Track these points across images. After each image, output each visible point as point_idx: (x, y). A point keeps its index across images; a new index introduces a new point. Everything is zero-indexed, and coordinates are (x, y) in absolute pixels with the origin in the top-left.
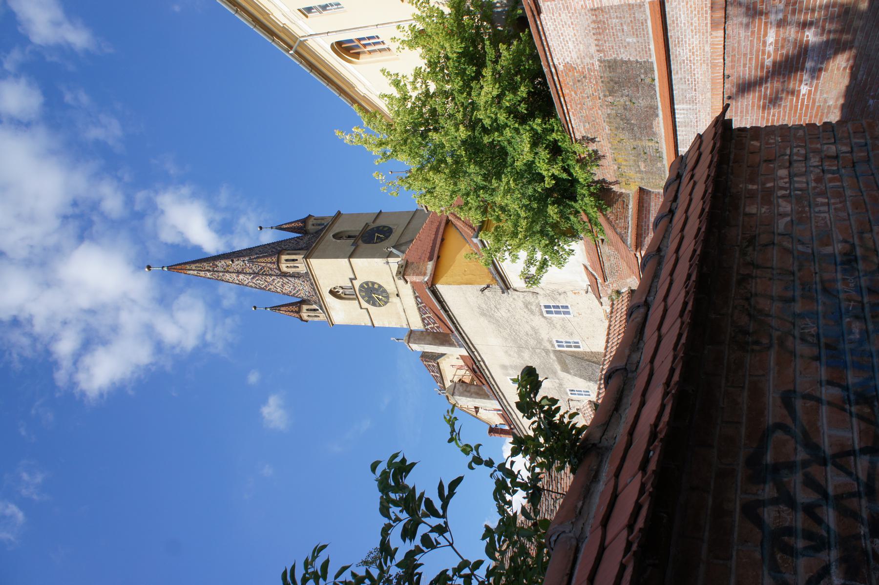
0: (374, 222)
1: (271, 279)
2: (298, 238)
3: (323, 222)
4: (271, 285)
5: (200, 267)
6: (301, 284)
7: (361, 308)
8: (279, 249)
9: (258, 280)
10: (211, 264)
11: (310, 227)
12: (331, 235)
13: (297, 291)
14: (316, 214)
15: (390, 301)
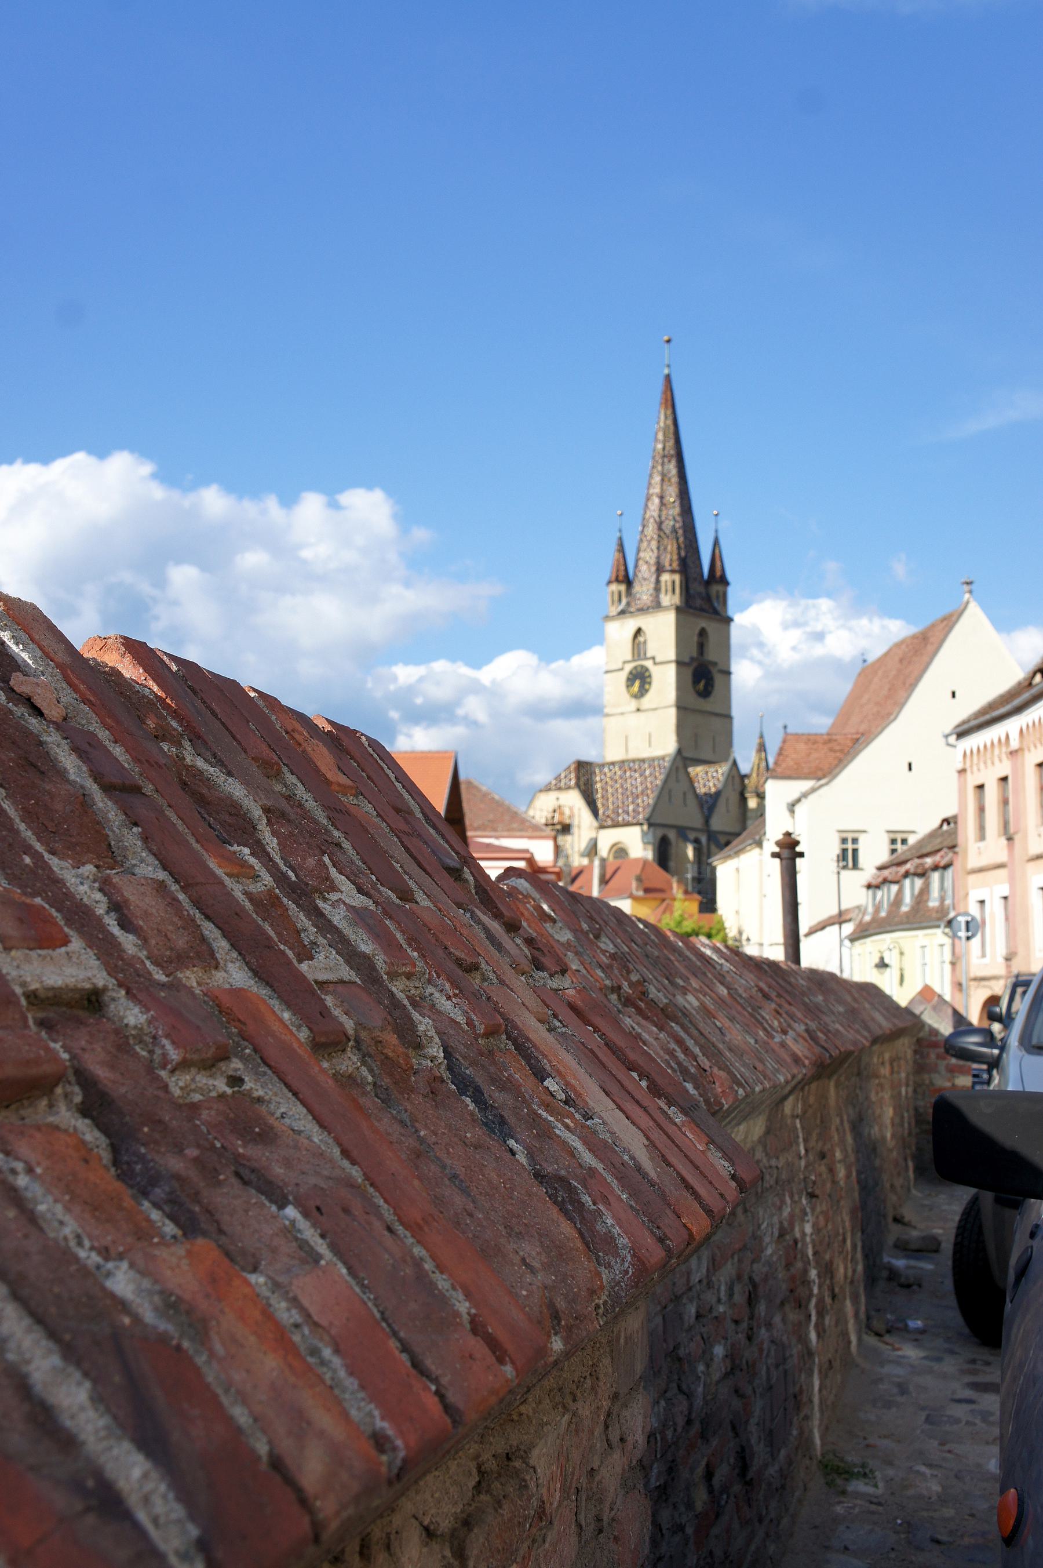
7: (625, 662)
11: (715, 588)
14: (731, 590)
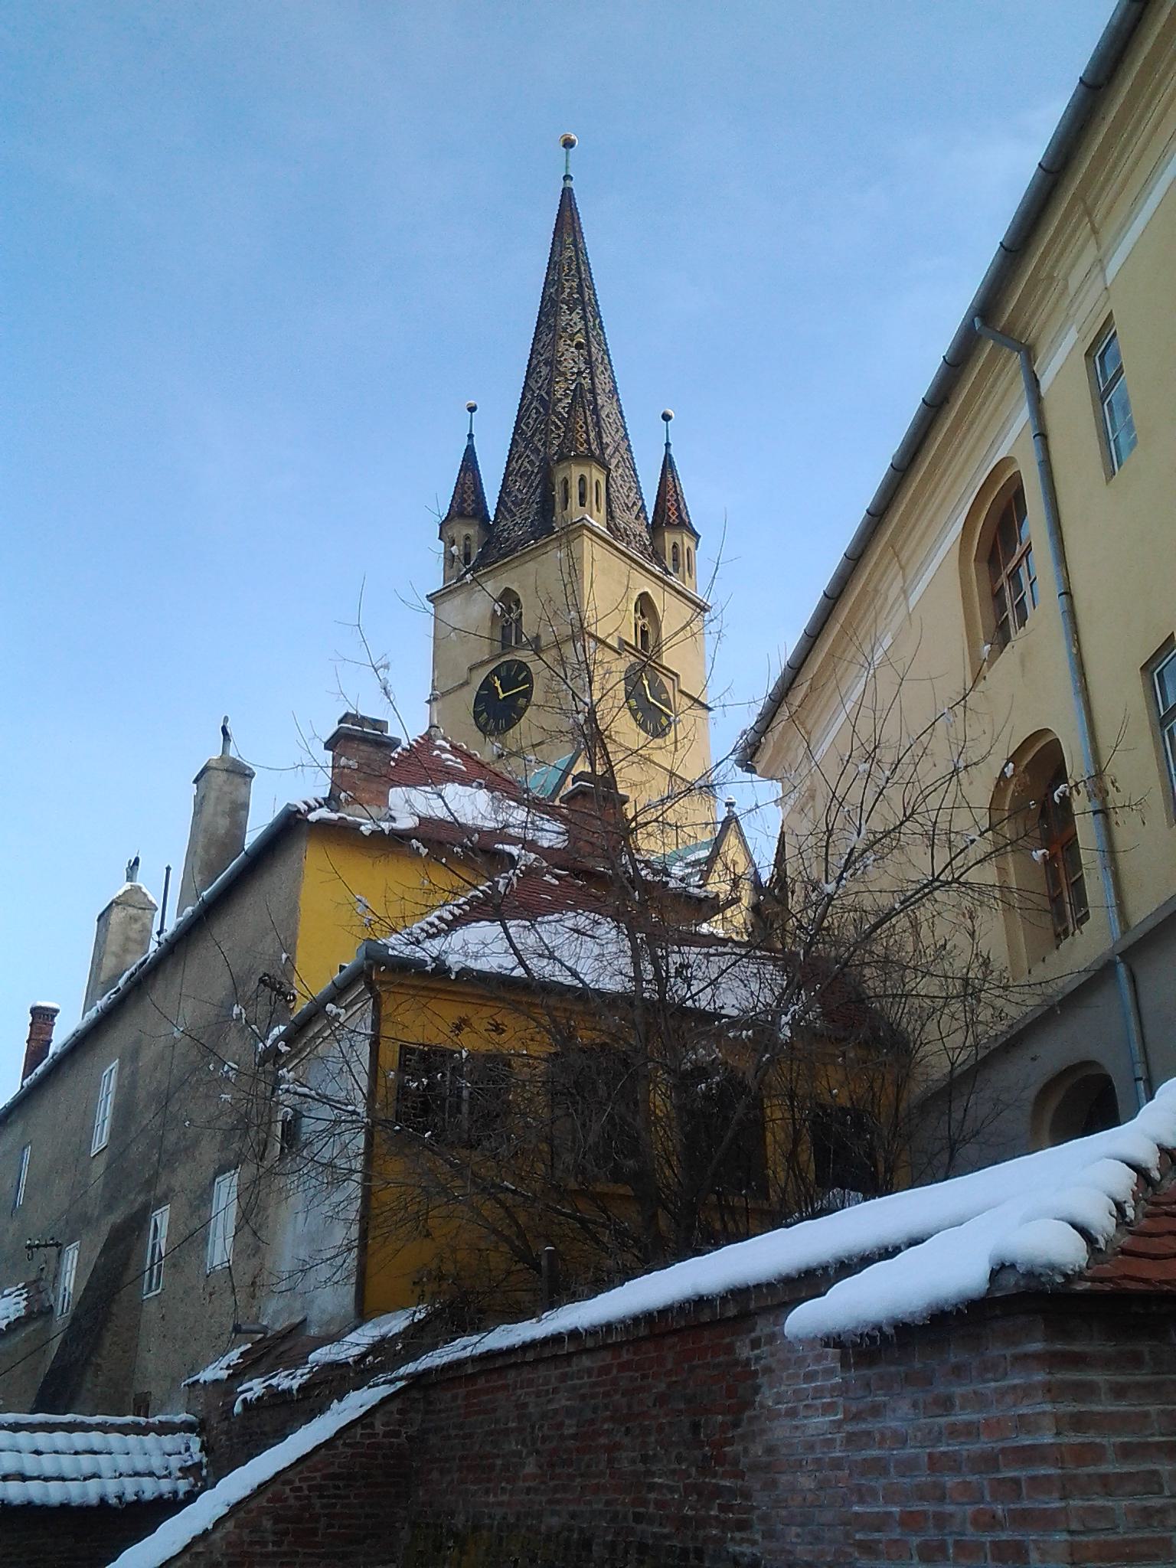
0: (681, 692)
2: (643, 508)
4: (526, 447)
5: (570, 270)
6: (526, 519)
8: (614, 462)
9: (538, 412)
12: (647, 589)
13: (510, 511)
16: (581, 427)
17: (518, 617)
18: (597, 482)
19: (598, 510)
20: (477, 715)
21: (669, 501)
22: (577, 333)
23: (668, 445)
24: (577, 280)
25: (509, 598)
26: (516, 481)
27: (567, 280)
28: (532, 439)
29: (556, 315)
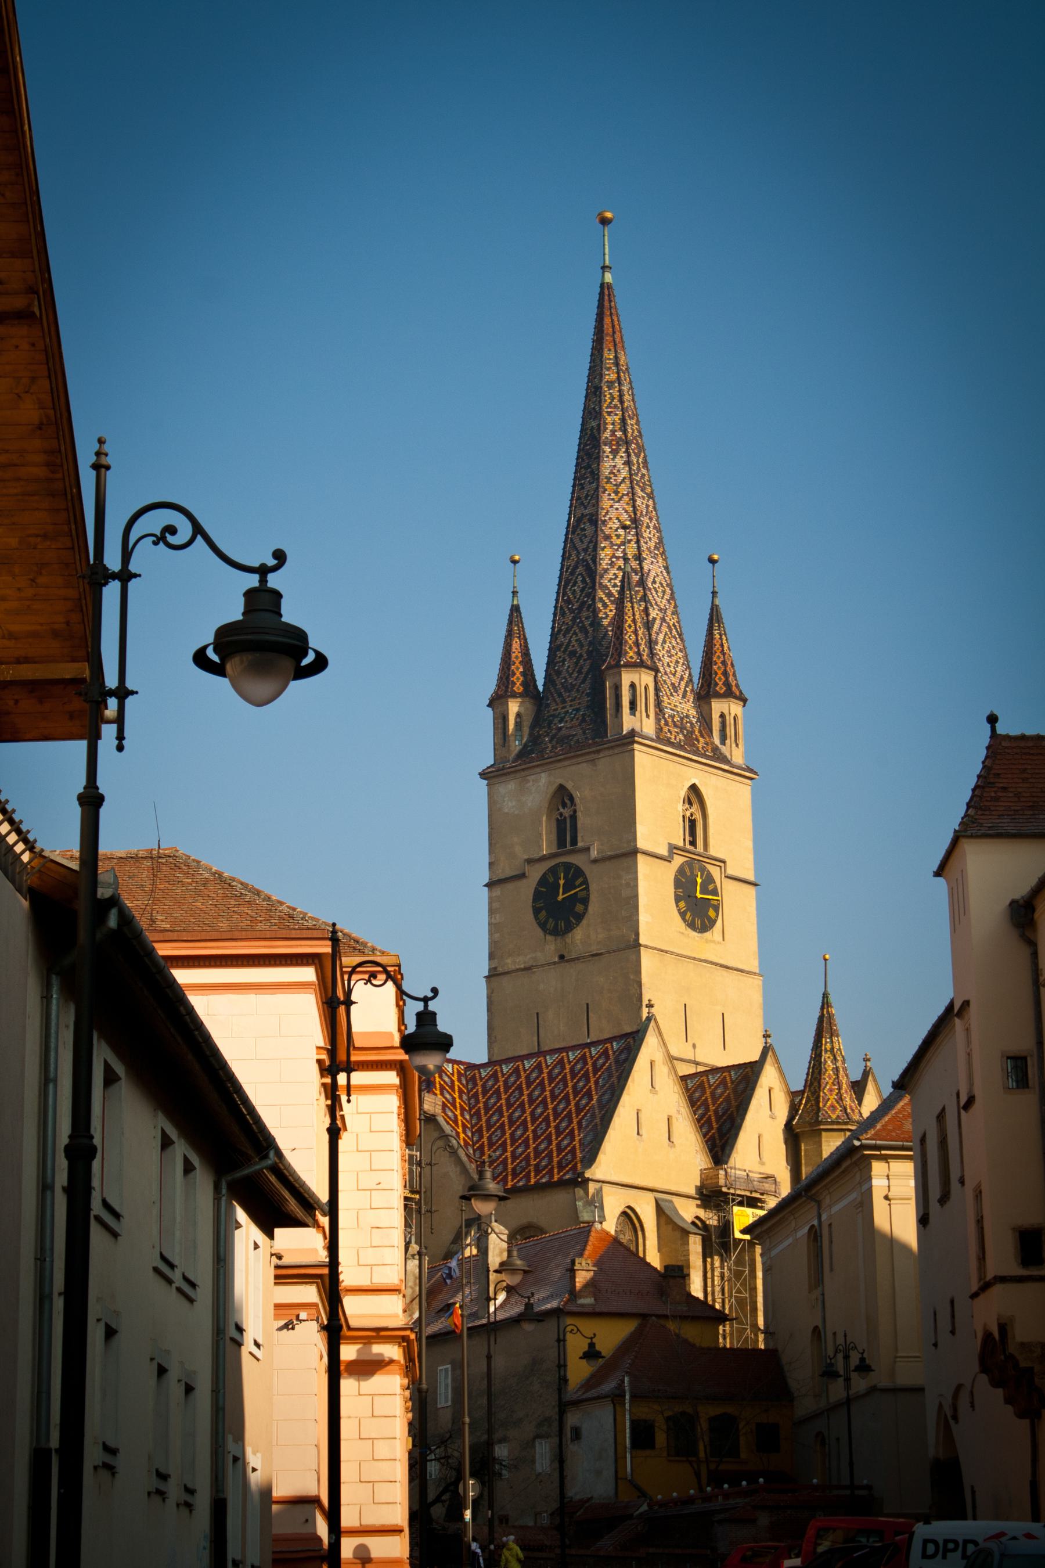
1: (587, 623)
3: (728, 742)
4: (574, 619)
6: (578, 710)
7: (530, 861)
8: (661, 637)
9: (584, 581)
10: (619, 434)
11: (718, 707)
12: (693, 781)
13: (560, 695)
15: (549, 938)
16: (630, 626)
17: (572, 813)
18: (646, 688)
19: (648, 716)
20: (536, 911)
21: (716, 664)
22: (621, 483)
23: (714, 594)
24: (619, 413)
25: (563, 796)
26: (564, 660)
27: (609, 413)
28: (579, 613)
29: (598, 459)
